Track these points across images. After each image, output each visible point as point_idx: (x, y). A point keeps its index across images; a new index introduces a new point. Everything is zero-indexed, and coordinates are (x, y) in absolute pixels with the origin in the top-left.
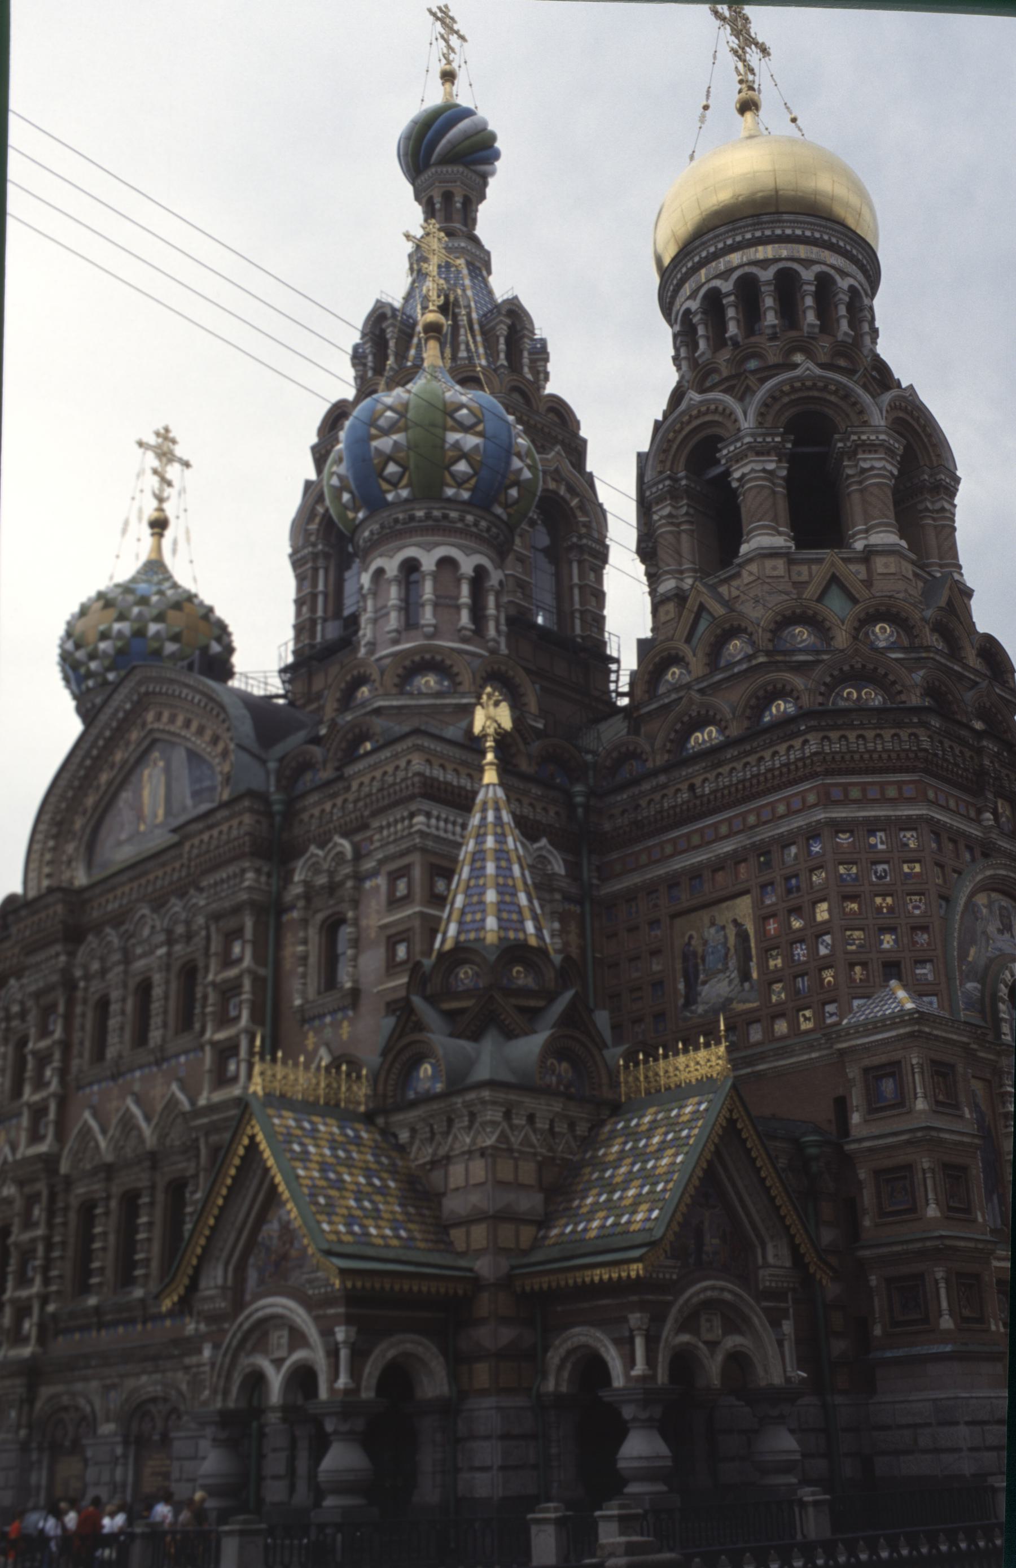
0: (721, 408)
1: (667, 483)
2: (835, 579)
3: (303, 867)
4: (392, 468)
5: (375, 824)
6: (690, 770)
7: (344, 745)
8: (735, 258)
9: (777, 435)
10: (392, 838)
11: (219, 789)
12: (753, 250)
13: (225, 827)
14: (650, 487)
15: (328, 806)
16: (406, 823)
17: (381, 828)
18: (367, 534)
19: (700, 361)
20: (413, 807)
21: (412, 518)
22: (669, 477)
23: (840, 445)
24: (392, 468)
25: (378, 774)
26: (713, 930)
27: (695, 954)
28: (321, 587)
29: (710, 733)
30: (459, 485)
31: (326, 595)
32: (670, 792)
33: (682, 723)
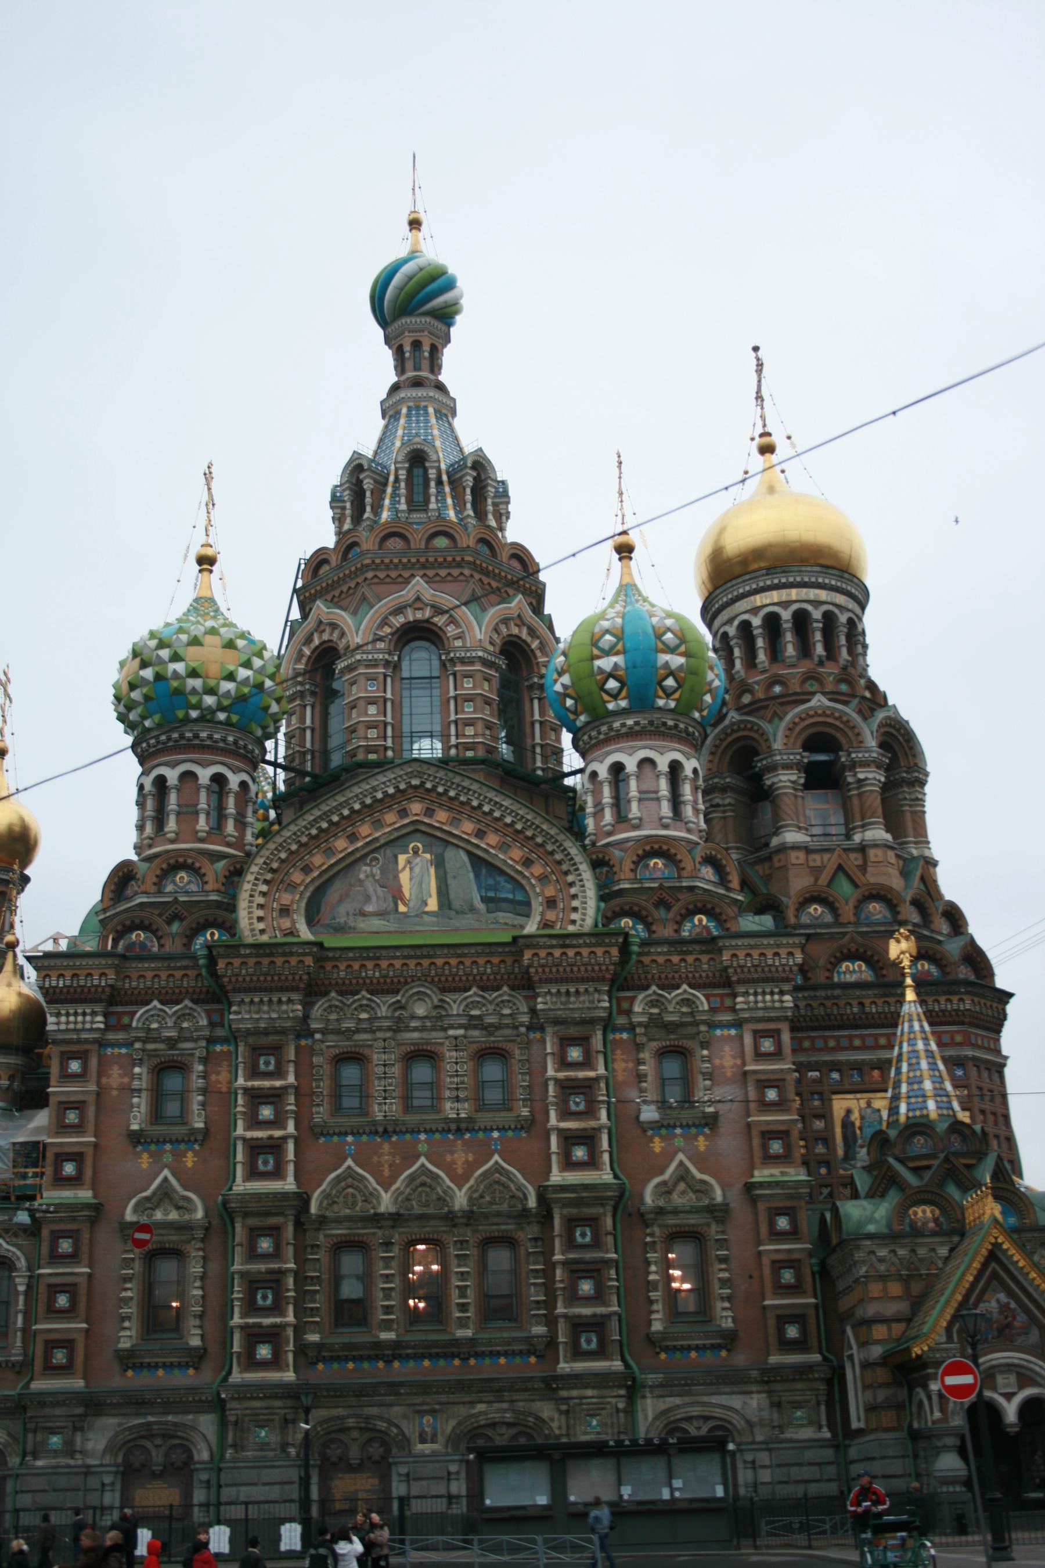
0: (845, 719)
1: (798, 757)
2: (922, 879)
3: (641, 1001)
4: (670, 682)
5: (741, 989)
6: (864, 993)
7: (683, 912)
8: (823, 595)
9: (887, 757)
10: (760, 1005)
11: (537, 906)
12: (833, 594)
13: (585, 952)
14: (780, 754)
15: (676, 959)
16: (776, 997)
17: (746, 994)
18: (630, 722)
20: (786, 987)
21: (676, 726)
22: (800, 754)
23: (905, 775)
24: (670, 682)
25: (755, 954)
26: (869, 1111)
27: (853, 1124)
28: (389, 695)
29: (860, 966)
30: (701, 711)
32: (842, 1003)
33: (842, 952)
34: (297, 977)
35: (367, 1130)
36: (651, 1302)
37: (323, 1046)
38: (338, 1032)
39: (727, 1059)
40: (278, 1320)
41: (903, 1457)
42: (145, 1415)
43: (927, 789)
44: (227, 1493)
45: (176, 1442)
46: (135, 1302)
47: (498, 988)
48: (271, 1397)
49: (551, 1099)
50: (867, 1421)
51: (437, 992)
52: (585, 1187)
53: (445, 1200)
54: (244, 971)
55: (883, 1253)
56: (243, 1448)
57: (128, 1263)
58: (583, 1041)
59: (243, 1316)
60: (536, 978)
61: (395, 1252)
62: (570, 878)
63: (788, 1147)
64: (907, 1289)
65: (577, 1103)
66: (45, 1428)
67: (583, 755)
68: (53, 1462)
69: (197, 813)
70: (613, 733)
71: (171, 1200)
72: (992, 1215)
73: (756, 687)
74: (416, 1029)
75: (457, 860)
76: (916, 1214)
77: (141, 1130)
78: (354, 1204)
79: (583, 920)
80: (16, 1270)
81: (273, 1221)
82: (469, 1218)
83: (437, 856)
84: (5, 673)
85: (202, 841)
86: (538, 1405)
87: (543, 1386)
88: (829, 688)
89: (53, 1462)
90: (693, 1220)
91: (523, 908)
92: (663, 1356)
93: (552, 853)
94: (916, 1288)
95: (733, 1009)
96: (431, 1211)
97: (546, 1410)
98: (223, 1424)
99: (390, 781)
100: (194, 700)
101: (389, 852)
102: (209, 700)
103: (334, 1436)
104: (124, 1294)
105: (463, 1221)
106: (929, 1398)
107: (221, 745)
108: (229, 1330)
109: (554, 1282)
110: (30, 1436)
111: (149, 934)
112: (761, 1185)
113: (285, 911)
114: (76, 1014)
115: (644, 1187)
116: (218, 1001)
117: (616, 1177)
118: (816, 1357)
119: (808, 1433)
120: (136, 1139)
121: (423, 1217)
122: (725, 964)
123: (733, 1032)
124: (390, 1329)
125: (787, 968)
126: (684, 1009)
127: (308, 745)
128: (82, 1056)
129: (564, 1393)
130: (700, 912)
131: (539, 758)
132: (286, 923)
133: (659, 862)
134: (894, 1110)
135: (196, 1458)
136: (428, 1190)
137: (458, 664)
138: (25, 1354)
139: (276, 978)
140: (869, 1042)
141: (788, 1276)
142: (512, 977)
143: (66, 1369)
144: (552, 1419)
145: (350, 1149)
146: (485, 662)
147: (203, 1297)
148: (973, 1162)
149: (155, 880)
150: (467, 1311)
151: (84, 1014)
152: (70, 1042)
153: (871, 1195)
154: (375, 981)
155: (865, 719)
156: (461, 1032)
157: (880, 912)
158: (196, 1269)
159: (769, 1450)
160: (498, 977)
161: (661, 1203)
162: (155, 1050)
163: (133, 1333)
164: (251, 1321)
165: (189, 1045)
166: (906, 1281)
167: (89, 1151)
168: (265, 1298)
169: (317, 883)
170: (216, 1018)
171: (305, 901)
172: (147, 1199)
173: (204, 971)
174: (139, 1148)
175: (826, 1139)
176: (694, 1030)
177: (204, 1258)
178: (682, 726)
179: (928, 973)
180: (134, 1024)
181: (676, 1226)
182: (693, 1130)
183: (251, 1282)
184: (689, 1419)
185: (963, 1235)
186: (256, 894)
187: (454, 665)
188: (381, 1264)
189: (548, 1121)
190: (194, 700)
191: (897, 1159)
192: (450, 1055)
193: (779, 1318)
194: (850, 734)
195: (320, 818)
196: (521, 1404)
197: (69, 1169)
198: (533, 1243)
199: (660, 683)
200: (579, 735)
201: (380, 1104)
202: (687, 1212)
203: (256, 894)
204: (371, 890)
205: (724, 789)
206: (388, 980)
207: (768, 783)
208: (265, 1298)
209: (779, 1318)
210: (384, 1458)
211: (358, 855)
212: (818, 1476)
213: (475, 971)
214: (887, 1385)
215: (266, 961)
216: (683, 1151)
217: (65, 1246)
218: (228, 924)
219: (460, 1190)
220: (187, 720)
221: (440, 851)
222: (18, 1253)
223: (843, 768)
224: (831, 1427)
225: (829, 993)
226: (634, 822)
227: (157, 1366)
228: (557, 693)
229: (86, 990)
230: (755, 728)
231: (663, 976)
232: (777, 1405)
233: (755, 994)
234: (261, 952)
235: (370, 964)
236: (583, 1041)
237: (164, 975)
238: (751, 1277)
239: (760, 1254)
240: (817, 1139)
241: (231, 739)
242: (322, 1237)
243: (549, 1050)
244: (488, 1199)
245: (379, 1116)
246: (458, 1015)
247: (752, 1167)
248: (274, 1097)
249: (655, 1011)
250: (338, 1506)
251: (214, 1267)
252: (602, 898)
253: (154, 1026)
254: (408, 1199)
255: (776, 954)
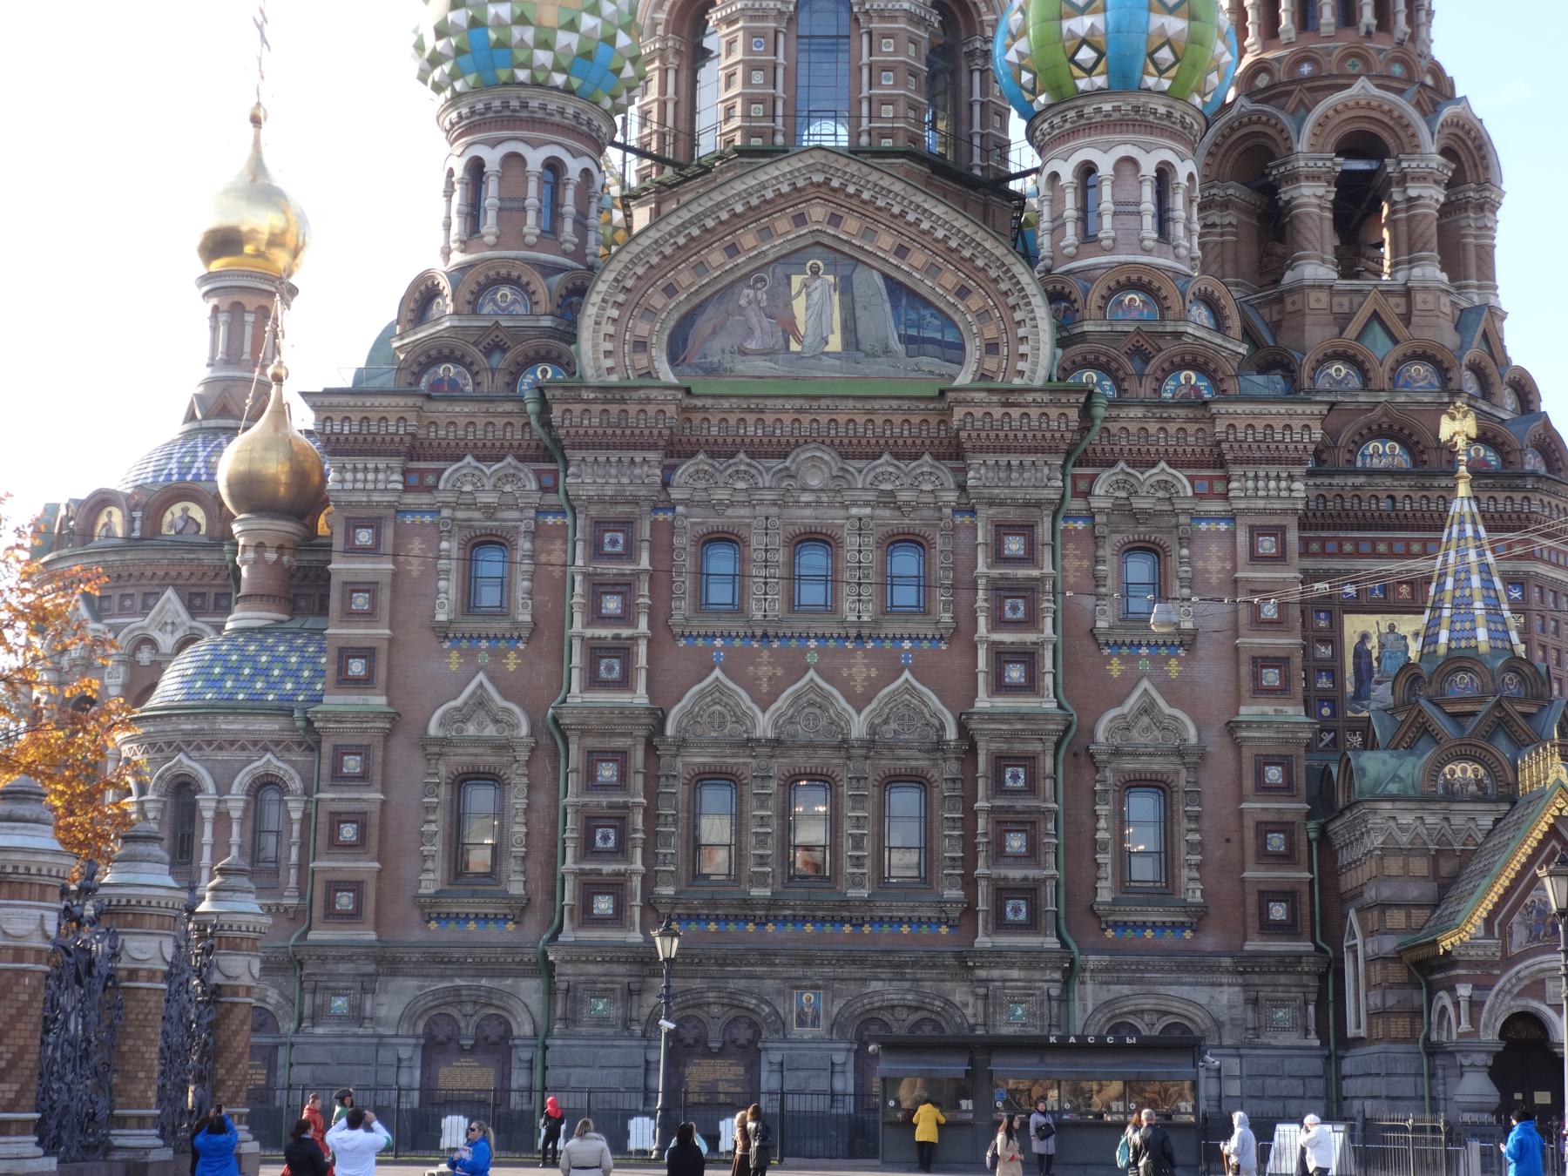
0: (1396, 114)
1: (1329, 164)
2: (1485, 335)
5: (1237, 471)
7: (1166, 366)
10: (1261, 493)
11: (973, 350)
16: (1283, 484)
18: (1107, 107)
19: (1323, 29)
20: (1298, 471)
21: (1169, 115)
24: (1165, 54)
25: (1259, 425)
26: (1391, 637)
27: (1369, 653)
28: (781, 58)
29: (1392, 449)
30: (1203, 95)
31: (785, 69)
33: (1370, 429)
34: (655, 432)
35: (742, 634)
36: (1098, 866)
37: (687, 523)
38: (708, 504)
39: (1213, 562)
40: (622, 867)
41: (1415, 1075)
42: (451, 977)
43: (1500, 214)
44: (553, 1076)
45: (492, 1011)
46: (438, 840)
47: (917, 457)
48: (611, 961)
49: (981, 603)
50: (1369, 1029)
51: (838, 458)
52: (1022, 717)
53: (838, 725)
54: (586, 422)
55: (1406, 819)
56: (575, 1022)
57: (430, 790)
58: (1026, 530)
59: (579, 859)
60: (968, 445)
61: (773, 786)
62: (1018, 316)
63: (1286, 679)
64: (1435, 868)
65: (1015, 609)
66: (327, 988)
67: (1041, 151)
68: (337, 1030)
69: (524, 210)
70: (1083, 122)
71: (489, 712)
72: (1558, 780)
73: (1277, 65)
74: (808, 505)
75: (870, 284)
76: (1453, 772)
77: (450, 622)
78: (722, 725)
79: (1034, 372)
80: (288, 792)
81: (619, 743)
82: (869, 749)
83: (842, 278)
84: (262, 12)
85: (531, 247)
86: (949, 985)
87: (953, 962)
88: (1378, 68)
89: (337, 1030)
90: (1157, 765)
91: (954, 351)
92: (1110, 933)
93: (996, 281)
94: (1446, 867)
95: (1225, 496)
96: (821, 739)
97: (960, 994)
98: (551, 992)
99: (784, 175)
100: (521, 56)
101: (780, 271)
102: (543, 57)
103: (689, 1012)
104: (426, 828)
105: (863, 752)
106: (1457, 1005)
107: (557, 118)
108: (559, 876)
109: (975, 835)
110: (308, 998)
111: (461, 369)
112: (1249, 725)
113: (641, 345)
114: (366, 469)
115: (1096, 721)
116: (552, 459)
117: (1060, 706)
118: (1305, 946)
119: (1293, 1039)
120: (443, 632)
121: (810, 746)
122: (1219, 437)
123: (1223, 526)
124: (765, 885)
125: (1300, 446)
126: (1160, 494)
127: (670, 122)
128: (374, 524)
129: (982, 973)
130: (1188, 366)
131: (977, 151)
132: (642, 361)
133: (1137, 298)
134: (1430, 638)
135: (515, 1032)
136: (818, 711)
137: (876, 19)
138: (302, 896)
139: (628, 432)
140: (1398, 548)
141: (1276, 842)
142: (937, 442)
143: (354, 916)
144: (966, 1005)
145: (718, 656)
146: (912, 18)
147: (527, 834)
148: (1534, 710)
149: (469, 297)
150: (861, 866)
151: (377, 470)
152: (359, 505)
153: (1393, 746)
154: (756, 440)
155: (1424, 114)
156: (868, 511)
157: (1425, 378)
158: (518, 801)
159: (1240, 1056)
160: (918, 442)
161: (1117, 741)
162: (469, 520)
163: (438, 875)
164: (587, 866)
165: (515, 514)
166: (1435, 858)
167: (384, 646)
168: (605, 838)
169: (684, 309)
170: (548, 481)
171: (667, 332)
172: (456, 709)
173: (533, 420)
174: (447, 645)
175: (1335, 672)
176: (1174, 521)
177: (529, 786)
178: (1177, 115)
179: (1484, 462)
180: (441, 486)
181: (1134, 771)
182: (1164, 651)
183: (589, 818)
184: (1139, 1013)
185: (1514, 803)
186: (604, 321)
187: (870, 19)
188: (755, 803)
189: (975, 631)
190: (521, 56)
191: (1430, 701)
192: (851, 541)
193: (1261, 894)
194: (1402, 134)
195: (690, 222)
196: (928, 984)
197: (357, 667)
198: (950, 785)
199: (1151, 55)
200: (1037, 122)
201: (759, 600)
202: (1150, 755)
203: (604, 321)
204: (754, 320)
205: (1225, 205)
206: (774, 441)
207: (1285, 197)
208: (605, 838)
209: (1261, 894)
210: (752, 1042)
211: (738, 274)
212: (1300, 1092)
213: (888, 433)
214: (1401, 985)
215: (615, 409)
216: (1149, 677)
217: (352, 764)
218: (564, 360)
219: (859, 712)
220: (512, 82)
221: (847, 272)
222: (292, 771)
223: (1389, 182)
224: (1321, 1032)
225: (1350, 481)
226: (1105, 243)
227: (467, 918)
228: (1010, 63)
229: (379, 439)
230: (1273, 122)
231: (1135, 449)
232: (1254, 1002)
233: (1256, 478)
234: (609, 396)
235: (751, 418)
236: (1026, 530)
237: (481, 422)
238: (1228, 840)
239: (1241, 812)
240: (1320, 671)
241: (570, 111)
242: (680, 765)
243: (980, 539)
244: (894, 726)
245: (758, 615)
246: (864, 489)
247: (1238, 702)
248: (623, 587)
249: (1123, 494)
250: (693, 1098)
251: (542, 798)
252: (1061, 343)
253: (468, 488)
254: (791, 721)
255: (1288, 427)
